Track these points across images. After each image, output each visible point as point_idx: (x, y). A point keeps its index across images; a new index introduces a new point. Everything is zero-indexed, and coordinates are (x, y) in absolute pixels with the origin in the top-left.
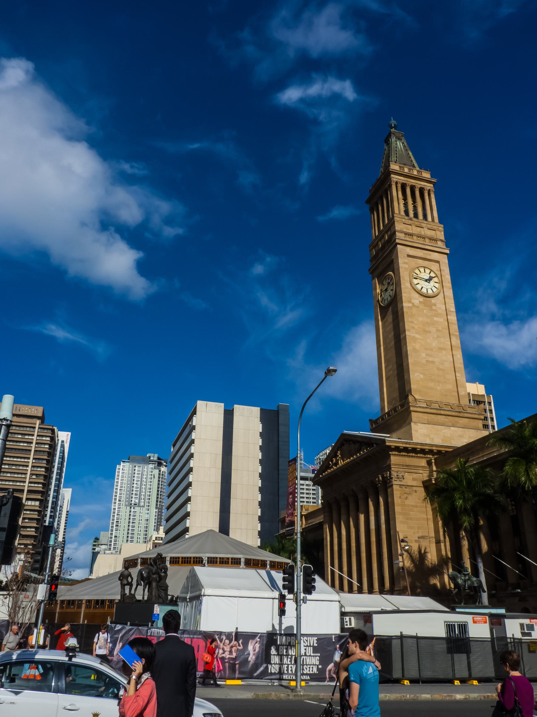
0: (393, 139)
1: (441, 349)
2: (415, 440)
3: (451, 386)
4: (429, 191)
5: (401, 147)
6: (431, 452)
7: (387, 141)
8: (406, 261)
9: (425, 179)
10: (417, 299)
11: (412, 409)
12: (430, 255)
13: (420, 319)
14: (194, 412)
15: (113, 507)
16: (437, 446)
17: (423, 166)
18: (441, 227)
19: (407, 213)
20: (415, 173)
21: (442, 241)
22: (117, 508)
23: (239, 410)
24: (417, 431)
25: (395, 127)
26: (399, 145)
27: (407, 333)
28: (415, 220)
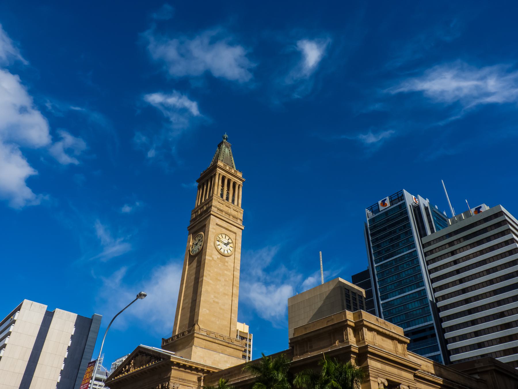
0: (224, 146)
1: (225, 294)
2: (192, 360)
3: (226, 323)
4: (239, 185)
6: (202, 371)
7: (219, 146)
8: (215, 227)
9: (238, 177)
10: (216, 256)
11: (195, 335)
13: (216, 270)
14: (19, 309)
16: (207, 367)
17: (239, 168)
18: (242, 211)
19: (222, 195)
20: (233, 171)
21: (240, 220)
23: (59, 313)
24: (195, 353)
25: (226, 139)
26: (226, 151)
27: (204, 278)
28: (226, 201)
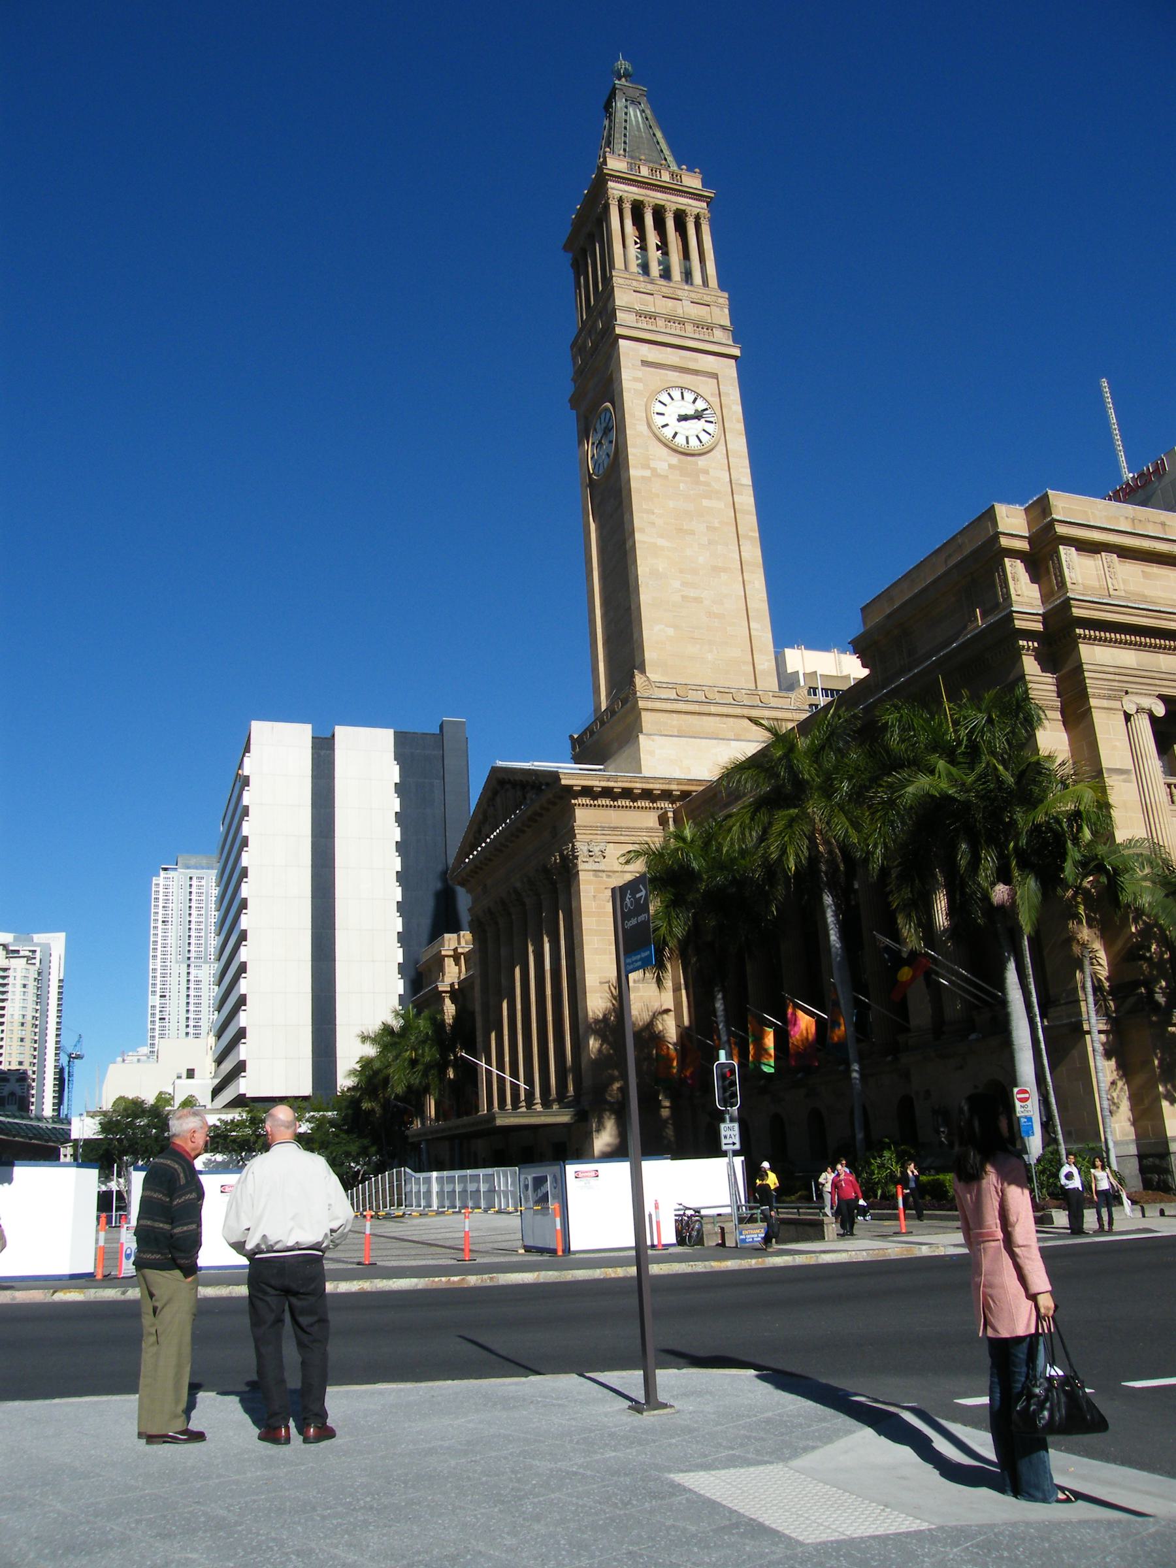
0: (620, 103)
1: (716, 570)
2: (646, 772)
3: (739, 652)
4: (697, 217)
5: (637, 121)
6: (667, 795)
7: (608, 106)
8: (640, 374)
9: (688, 191)
10: (663, 460)
11: (641, 704)
12: (696, 360)
13: (671, 504)
14: (247, 749)
15: (151, 967)
16: (679, 781)
17: (686, 159)
18: (723, 298)
19: (645, 268)
20: (666, 177)
21: (723, 327)
22: (159, 967)
23: (347, 738)
25: (627, 75)
26: (632, 115)
27: (638, 536)
28: (663, 282)
